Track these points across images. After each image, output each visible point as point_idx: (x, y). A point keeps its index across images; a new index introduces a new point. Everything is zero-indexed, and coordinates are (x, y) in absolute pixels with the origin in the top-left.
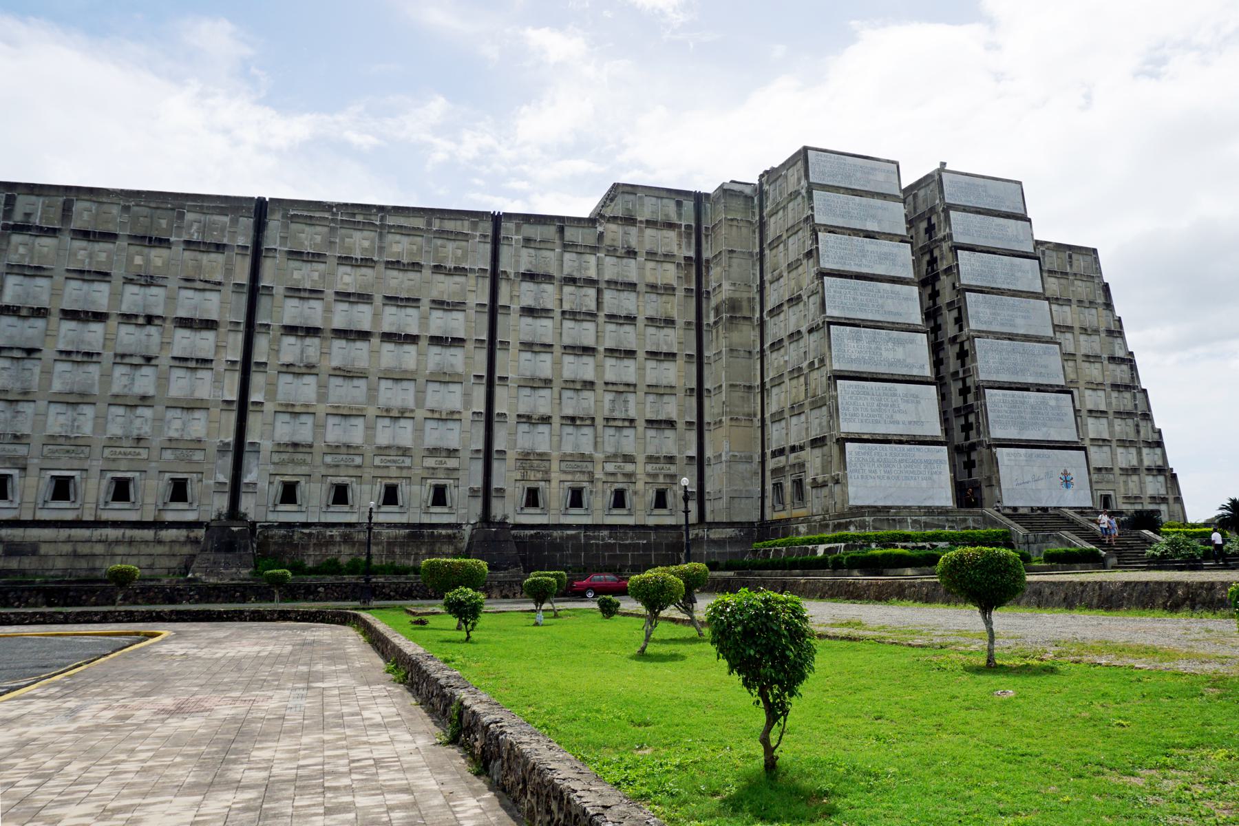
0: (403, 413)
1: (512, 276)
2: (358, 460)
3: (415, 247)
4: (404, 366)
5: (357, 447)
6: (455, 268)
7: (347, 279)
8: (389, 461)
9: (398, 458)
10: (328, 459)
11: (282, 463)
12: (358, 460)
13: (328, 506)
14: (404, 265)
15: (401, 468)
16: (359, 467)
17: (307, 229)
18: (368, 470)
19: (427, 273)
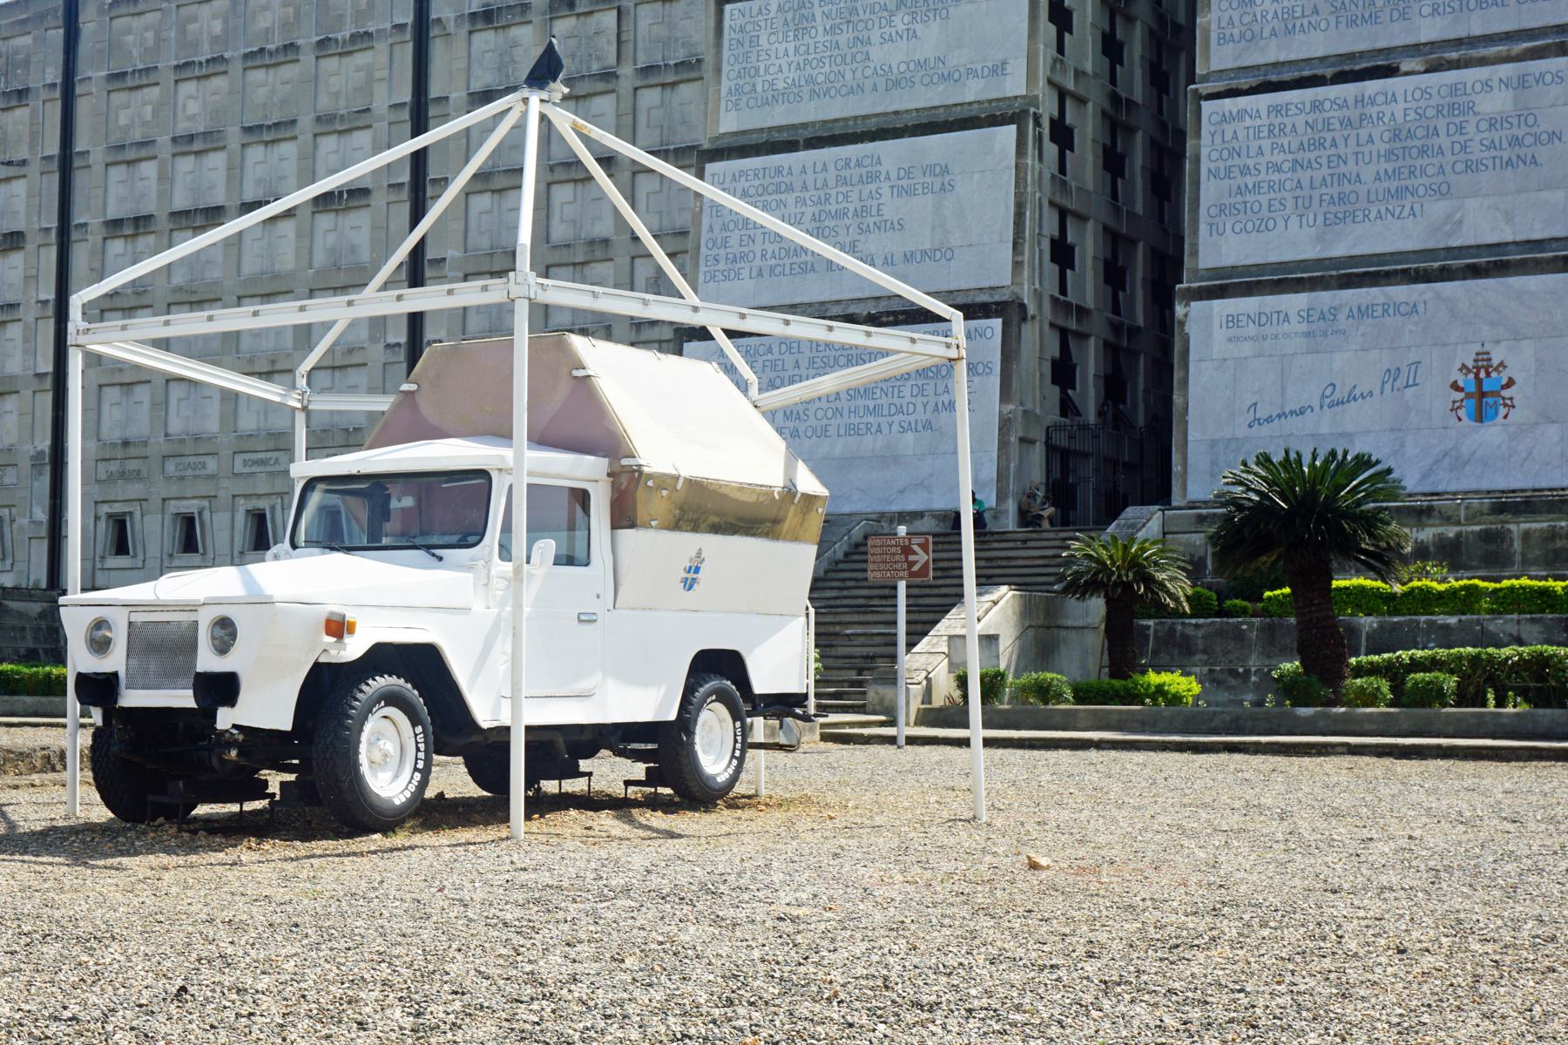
0: (273, 362)
1: (451, 27)
2: (212, 465)
3: (290, 10)
4: (277, 267)
5: (209, 439)
6: (352, 36)
7: (193, 108)
8: (256, 462)
9: (269, 455)
10: (171, 466)
11: (110, 479)
12: (212, 465)
13: (171, 556)
14: (271, 53)
15: (272, 474)
16: (211, 477)
17: (136, 23)
18: (225, 483)
19: (307, 58)
